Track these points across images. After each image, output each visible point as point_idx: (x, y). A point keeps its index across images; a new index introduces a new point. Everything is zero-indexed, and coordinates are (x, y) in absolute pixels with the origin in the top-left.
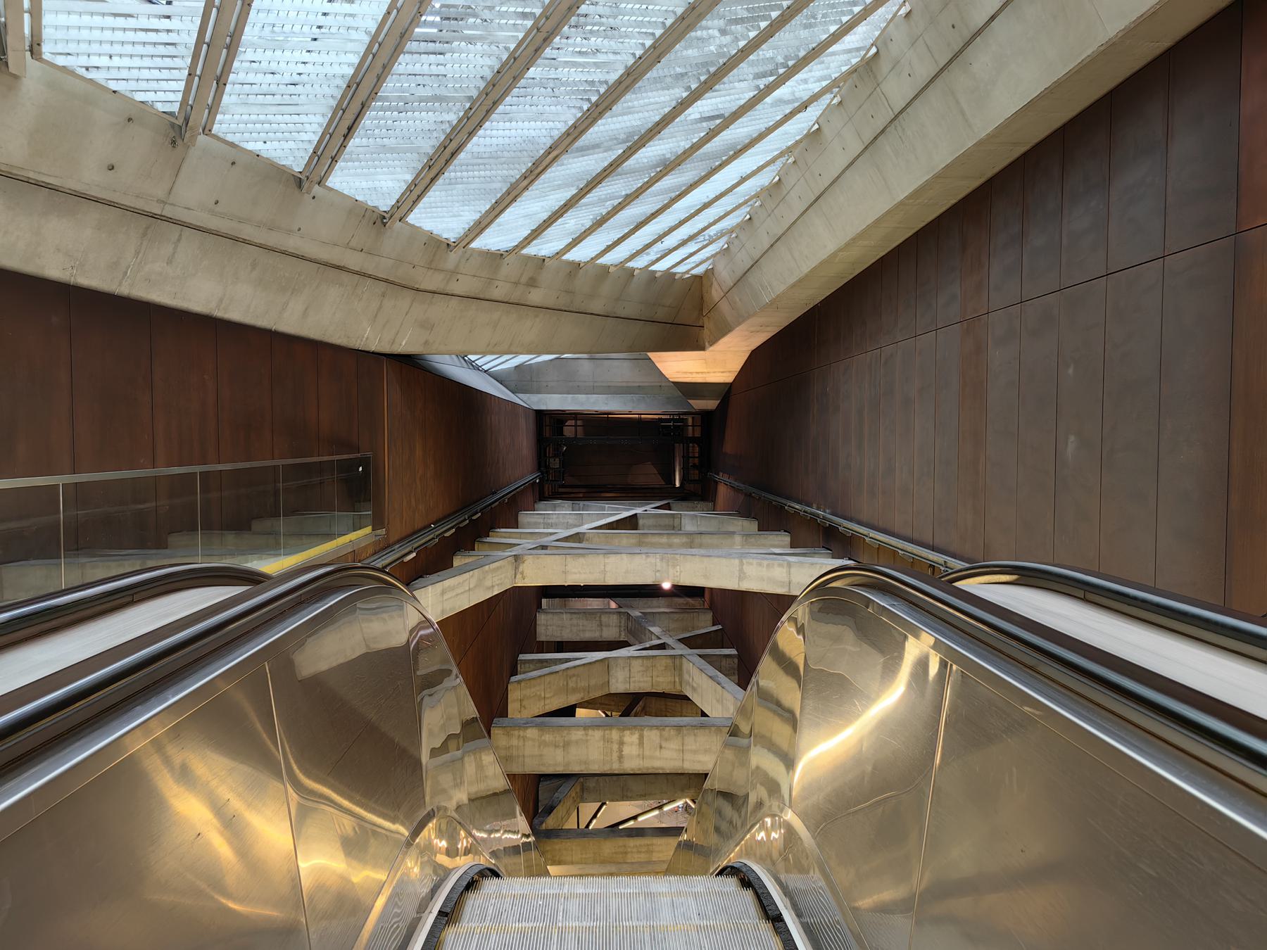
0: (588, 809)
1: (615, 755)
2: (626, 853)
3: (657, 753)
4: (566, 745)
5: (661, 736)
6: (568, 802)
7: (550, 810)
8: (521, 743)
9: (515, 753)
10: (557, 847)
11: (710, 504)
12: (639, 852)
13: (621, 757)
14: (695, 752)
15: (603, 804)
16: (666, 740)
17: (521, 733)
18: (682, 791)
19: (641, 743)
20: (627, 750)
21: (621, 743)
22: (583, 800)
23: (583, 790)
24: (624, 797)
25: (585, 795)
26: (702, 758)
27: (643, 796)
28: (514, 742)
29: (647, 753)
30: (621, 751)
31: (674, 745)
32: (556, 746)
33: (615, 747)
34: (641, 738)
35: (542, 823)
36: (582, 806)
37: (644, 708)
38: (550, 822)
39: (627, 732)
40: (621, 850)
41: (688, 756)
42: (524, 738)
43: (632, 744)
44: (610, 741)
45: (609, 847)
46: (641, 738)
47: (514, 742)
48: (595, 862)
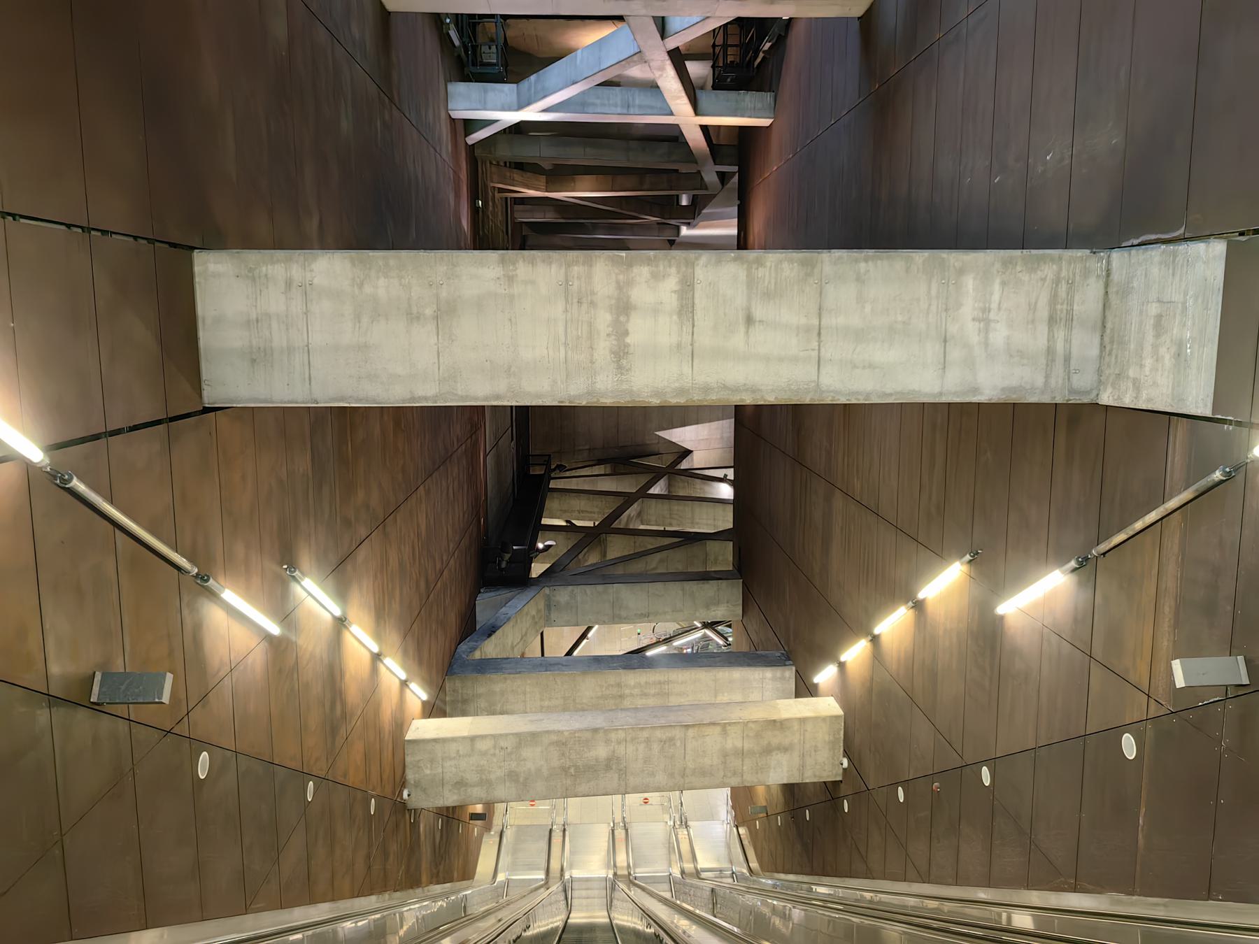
0: (559, 639)
1: (603, 348)
2: (621, 697)
3: (738, 341)
4: (445, 313)
5: (751, 282)
6: (525, 623)
7: (491, 631)
8: (297, 306)
9: (279, 340)
10: (498, 687)
11: (768, 97)
12: (645, 695)
13: (621, 353)
14: (859, 336)
15: (584, 636)
16: (768, 295)
17: (296, 272)
18: (707, 607)
19: (686, 309)
20: (639, 330)
21: (623, 308)
22: (549, 622)
23: (548, 607)
24: (616, 619)
25: (553, 616)
26: (881, 354)
27: (645, 616)
28: (274, 301)
29: (705, 339)
30: (621, 332)
31: (791, 313)
32: (413, 317)
33: (604, 319)
34: (687, 287)
35: (473, 649)
36: (547, 631)
37: (639, 514)
38: (490, 648)
39: (642, 272)
40: (614, 691)
41: (831, 350)
42: (306, 289)
43: (656, 311)
44: (585, 299)
45: (590, 686)
46: (687, 287)
47: (274, 301)
48: (565, 709)
